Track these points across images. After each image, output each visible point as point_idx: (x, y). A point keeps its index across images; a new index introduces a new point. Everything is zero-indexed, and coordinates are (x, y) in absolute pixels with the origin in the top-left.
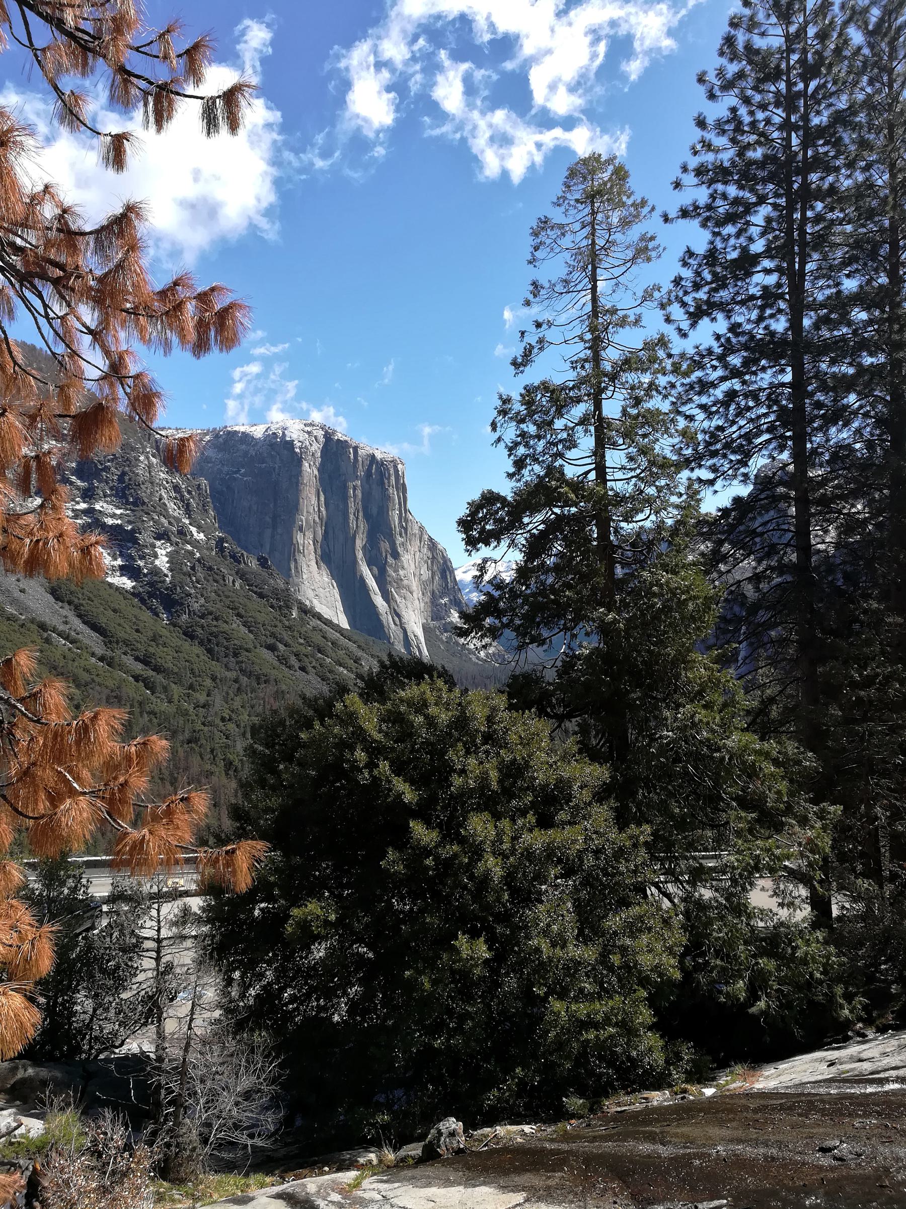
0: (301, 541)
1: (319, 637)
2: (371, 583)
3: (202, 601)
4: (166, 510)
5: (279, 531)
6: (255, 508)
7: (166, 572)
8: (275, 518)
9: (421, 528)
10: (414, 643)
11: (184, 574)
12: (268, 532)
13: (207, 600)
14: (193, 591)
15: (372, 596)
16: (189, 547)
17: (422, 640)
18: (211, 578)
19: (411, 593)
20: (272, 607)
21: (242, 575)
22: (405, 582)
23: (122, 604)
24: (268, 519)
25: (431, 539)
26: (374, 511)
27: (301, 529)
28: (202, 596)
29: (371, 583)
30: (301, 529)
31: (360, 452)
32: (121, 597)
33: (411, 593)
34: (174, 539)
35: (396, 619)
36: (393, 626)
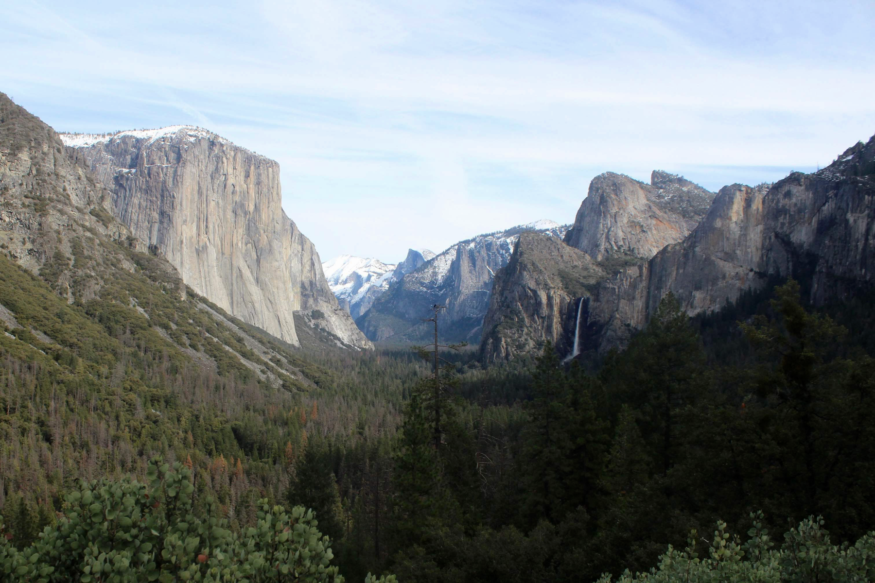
0: (184, 235)
1: (206, 318)
2: (247, 272)
3: (102, 283)
4: (69, 199)
5: (165, 225)
6: (144, 204)
7: (68, 255)
8: (162, 213)
9: (292, 225)
10: (285, 329)
11: (86, 258)
12: (156, 226)
13: (106, 281)
14: (93, 274)
15: (248, 285)
16: (88, 234)
17: (293, 326)
18: (109, 263)
19: (284, 283)
20: (165, 290)
21: (137, 260)
22: (278, 273)
23: (29, 284)
24: (156, 215)
25: (301, 236)
26: (252, 208)
27: (185, 221)
28: (102, 278)
29: (247, 272)
30: (185, 221)
31: (239, 155)
32: (29, 278)
33: (284, 283)
34: (75, 226)
35: (270, 305)
36: (266, 313)
